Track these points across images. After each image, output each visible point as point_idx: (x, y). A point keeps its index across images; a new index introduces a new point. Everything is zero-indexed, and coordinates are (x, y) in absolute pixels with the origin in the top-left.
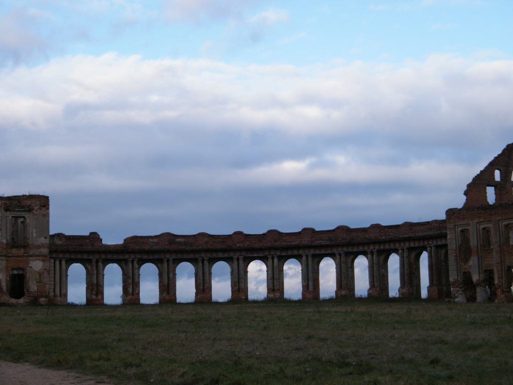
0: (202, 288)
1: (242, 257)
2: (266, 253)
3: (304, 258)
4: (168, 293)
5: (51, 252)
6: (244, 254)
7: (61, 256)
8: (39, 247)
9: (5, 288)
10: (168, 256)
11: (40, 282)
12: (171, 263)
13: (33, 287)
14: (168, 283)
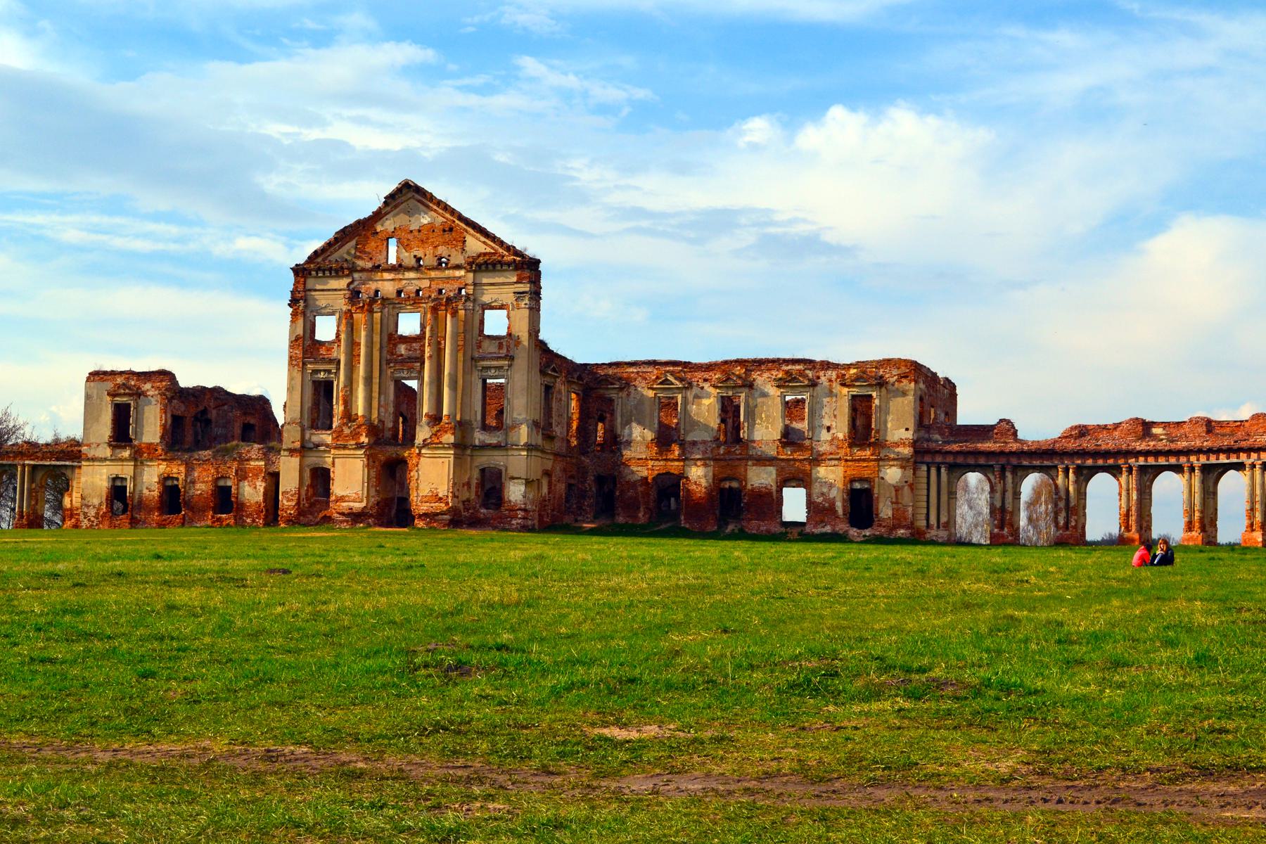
5: (916, 452)
7: (939, 459)
8: (897, 444)
9: (840, 511)
11: (897, 503)
13: (885, 511)
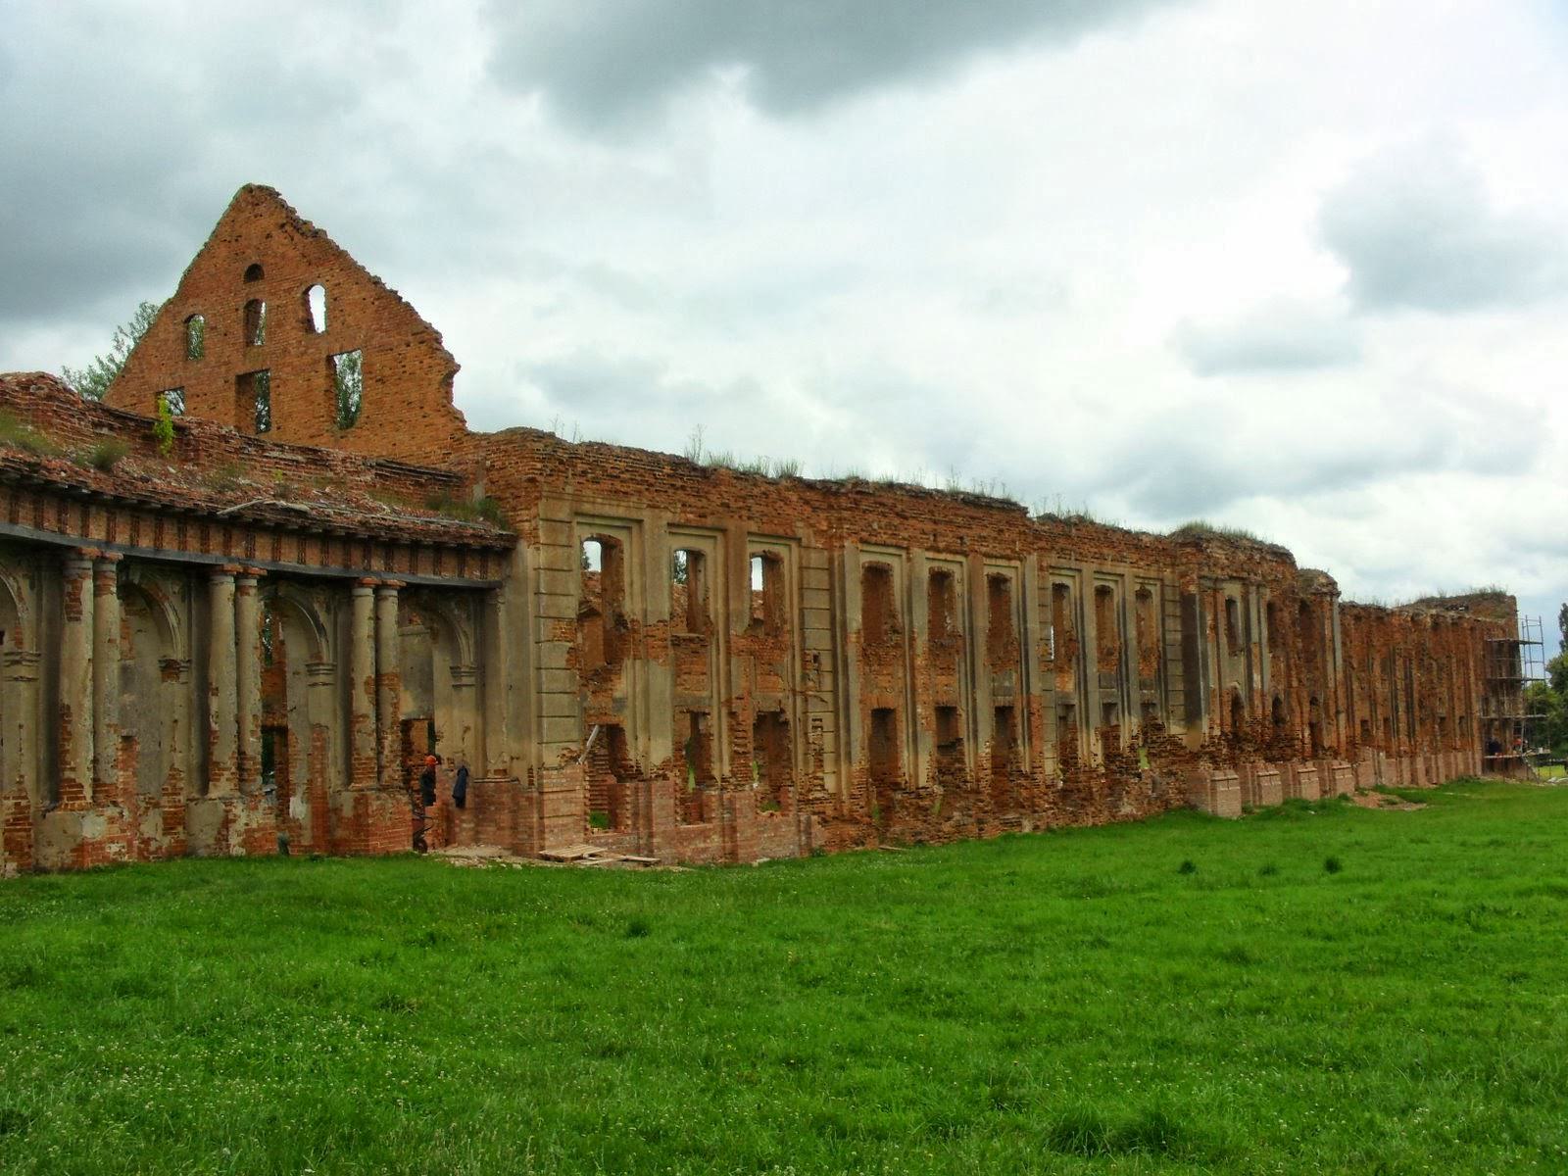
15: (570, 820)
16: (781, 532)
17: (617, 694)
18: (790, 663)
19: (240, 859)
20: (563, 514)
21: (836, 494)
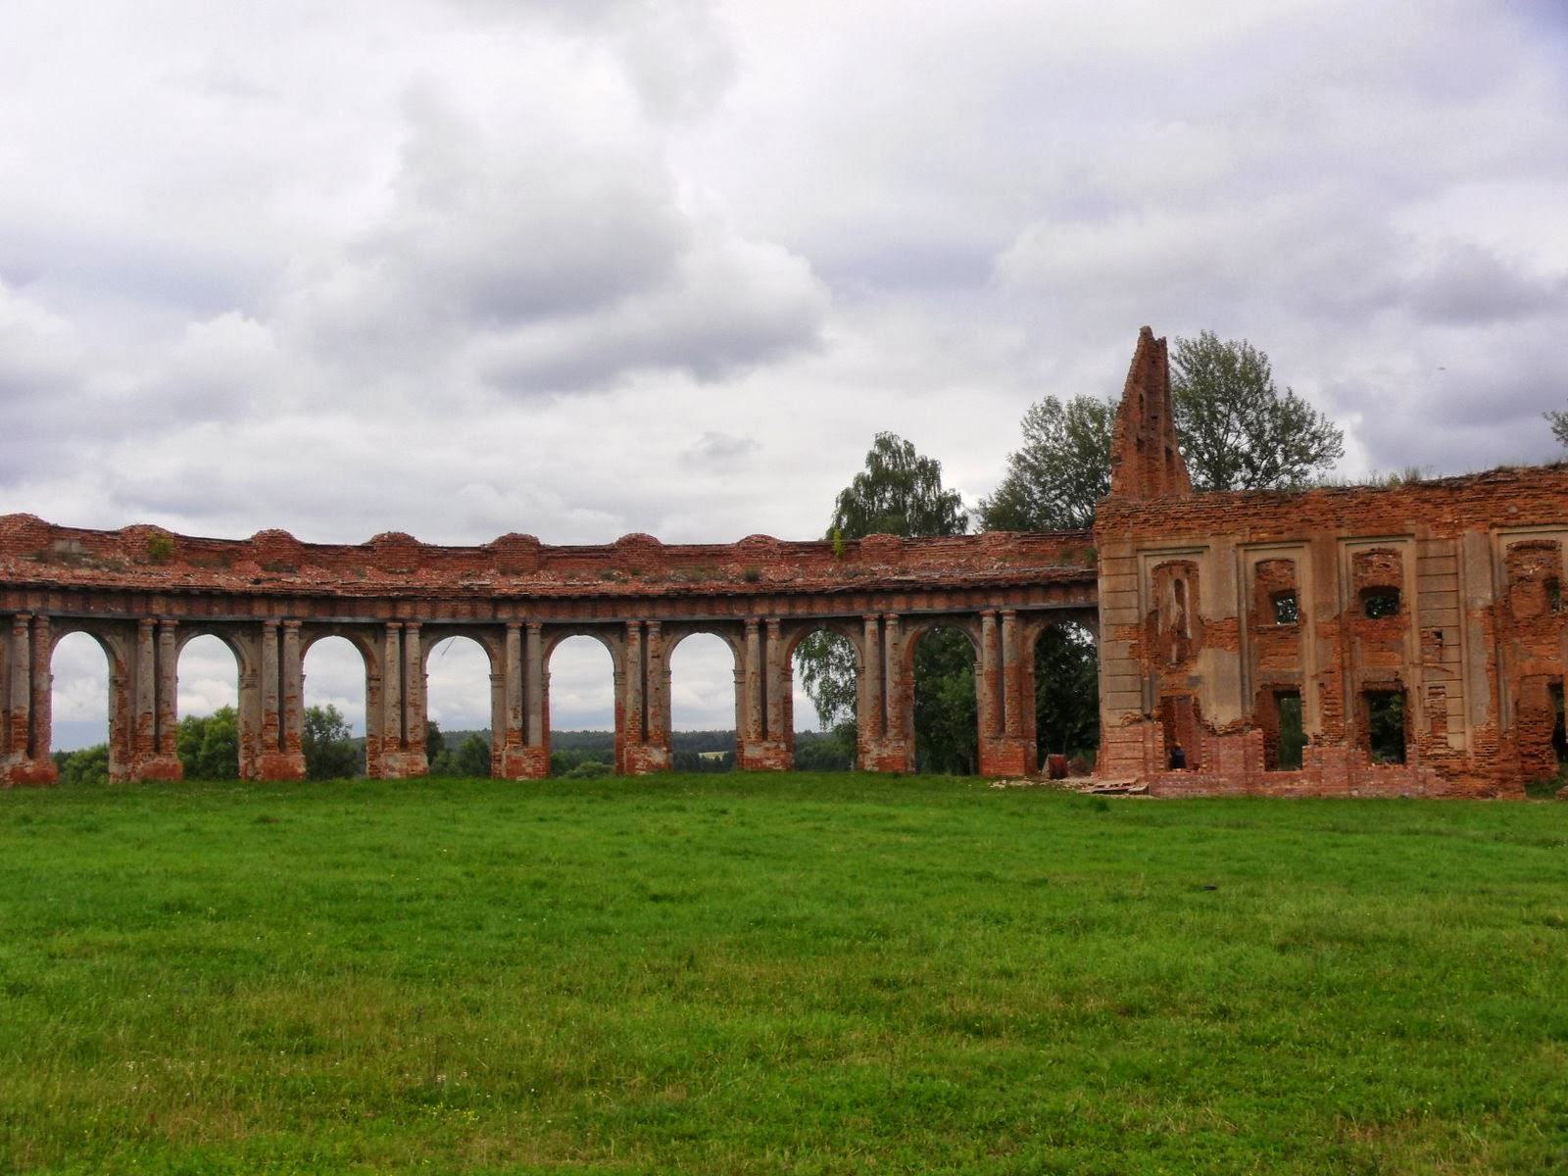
0: (151, 732)
1: (298, 623)
2: (383, 614)
3: (513, 636)
4: (31, 753)
6: (302, 611)
10: (33, 604)
12: (43, 633)
14: (32, 714)
15: (1133, 761)
16: (1384, 531)
17: (1193, 674)
18: (1412, 640)
19: (871, 773)
20: (1125, 551)
21: (1460, 488)
